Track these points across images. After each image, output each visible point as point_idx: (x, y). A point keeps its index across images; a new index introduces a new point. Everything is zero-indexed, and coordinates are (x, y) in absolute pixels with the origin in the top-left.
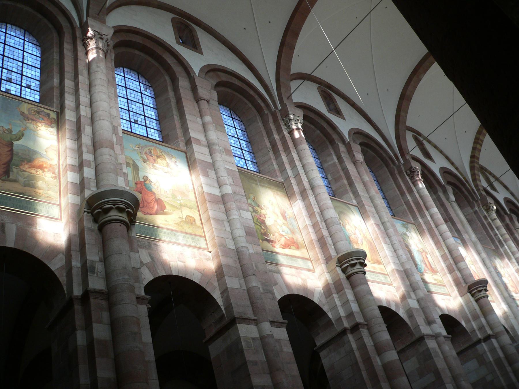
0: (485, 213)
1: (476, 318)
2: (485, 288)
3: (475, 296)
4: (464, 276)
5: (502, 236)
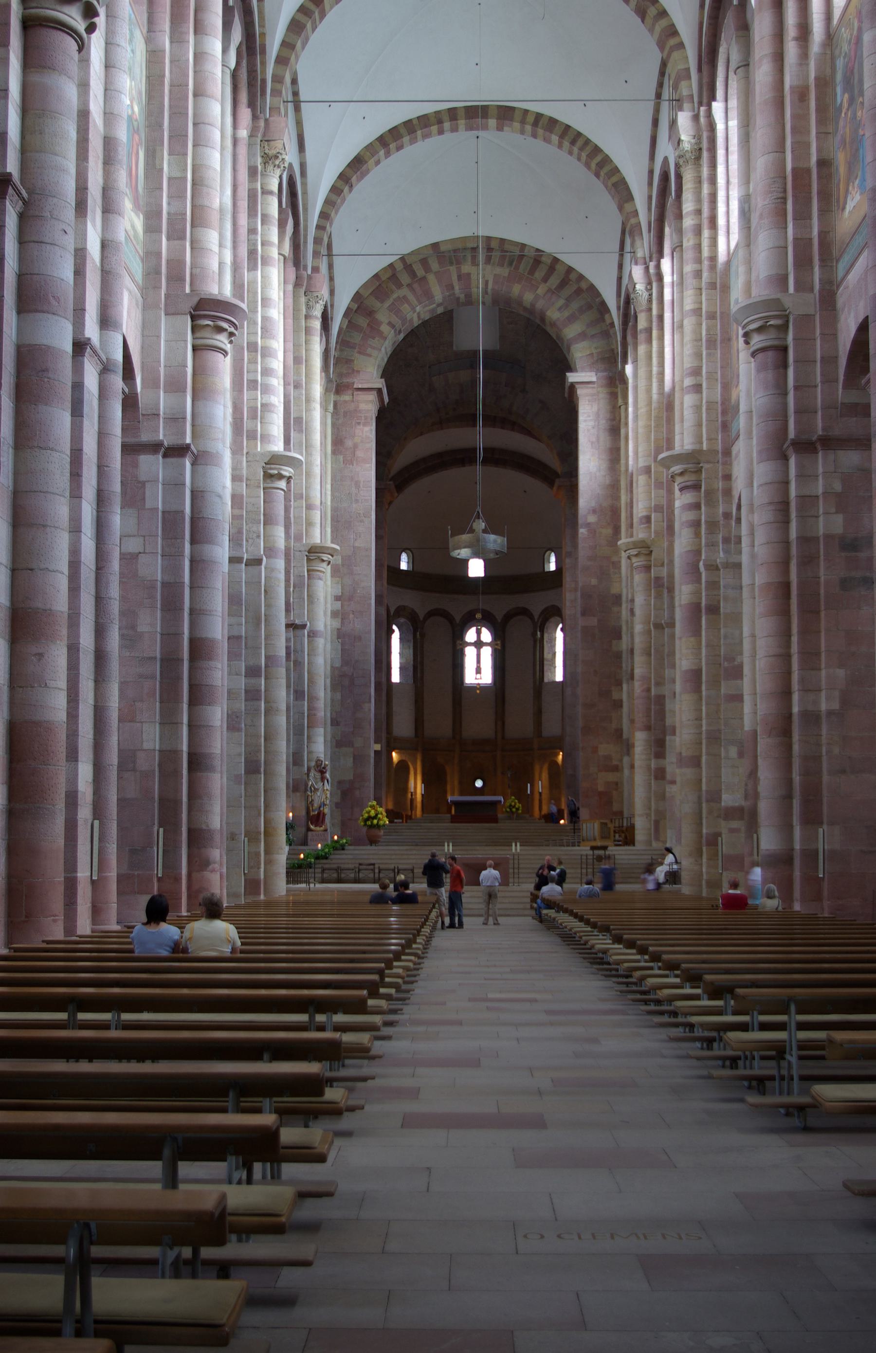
0: (259, 160)
1: (175, 386)
2: (232, 329)
3: (198, 335)
4: (198, 270)
5: (262, 244)
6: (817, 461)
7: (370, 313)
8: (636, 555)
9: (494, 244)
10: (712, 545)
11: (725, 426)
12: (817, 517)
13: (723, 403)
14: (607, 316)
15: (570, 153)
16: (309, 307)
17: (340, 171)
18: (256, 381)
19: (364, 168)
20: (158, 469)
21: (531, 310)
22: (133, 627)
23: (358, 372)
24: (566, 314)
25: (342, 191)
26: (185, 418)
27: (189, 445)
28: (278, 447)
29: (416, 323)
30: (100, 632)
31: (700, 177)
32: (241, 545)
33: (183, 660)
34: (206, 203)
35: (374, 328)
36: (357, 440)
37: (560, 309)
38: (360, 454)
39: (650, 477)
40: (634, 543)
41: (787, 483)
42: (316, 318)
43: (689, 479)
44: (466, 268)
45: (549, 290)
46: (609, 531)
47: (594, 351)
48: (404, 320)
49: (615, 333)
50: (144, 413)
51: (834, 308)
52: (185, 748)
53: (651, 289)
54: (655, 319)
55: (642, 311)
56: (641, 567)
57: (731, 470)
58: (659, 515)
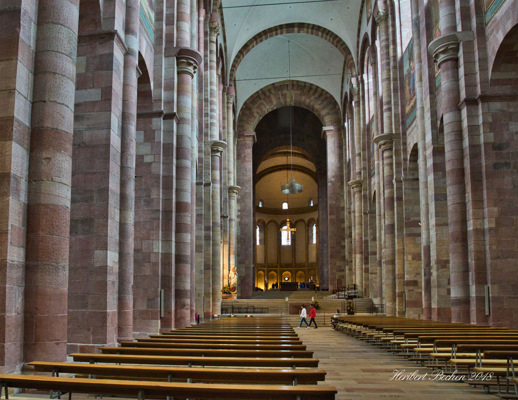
3: (180, 67)
4: (180, 39)
6: (477, 109)
7: (250, 109)
8: (356, 187)
9: (295, 83)
10: (398, 172)
11: (403, 123)
12: (479, 135)
13: (402, 114)
14: (337, 106)
15: (326, 39)
16: (228, 99)
17: (239, 50)
18: (208, 113)
19: (248, 48)
20: (161, 124)
21: (309, 106)
22: (149, 196)
23: (246, 130)
24: (322, 106)
25: (240, 57)
26: (173, 102)
27: (175, 113)
28: (217, 138)
29: (266, 113)
30: (123, 184)
31: (388, 26)
32: (202, 178)
33: (172, 211)
34: (183, 11)
35: (252, 115)
36: (246, 154)
37: (319, 104)
38: (247, 159)
39: (361, 157)
40: (355, 182)
41: (459, 122)
42: (231, 103)
43: (387, 146)
44: (285, 92)
45: (316, 98)
46: (340, 184)
47: (332, 119)
48: (262, 111)
49: (340, 112)
50: (155, 99)
51: (484, 36)
52: (173, 252)
53: (359, 86)
54: (361, 97)
55: (355, 95)
56: (358, 191)
57: (406, 141)
58: (365, 171)
